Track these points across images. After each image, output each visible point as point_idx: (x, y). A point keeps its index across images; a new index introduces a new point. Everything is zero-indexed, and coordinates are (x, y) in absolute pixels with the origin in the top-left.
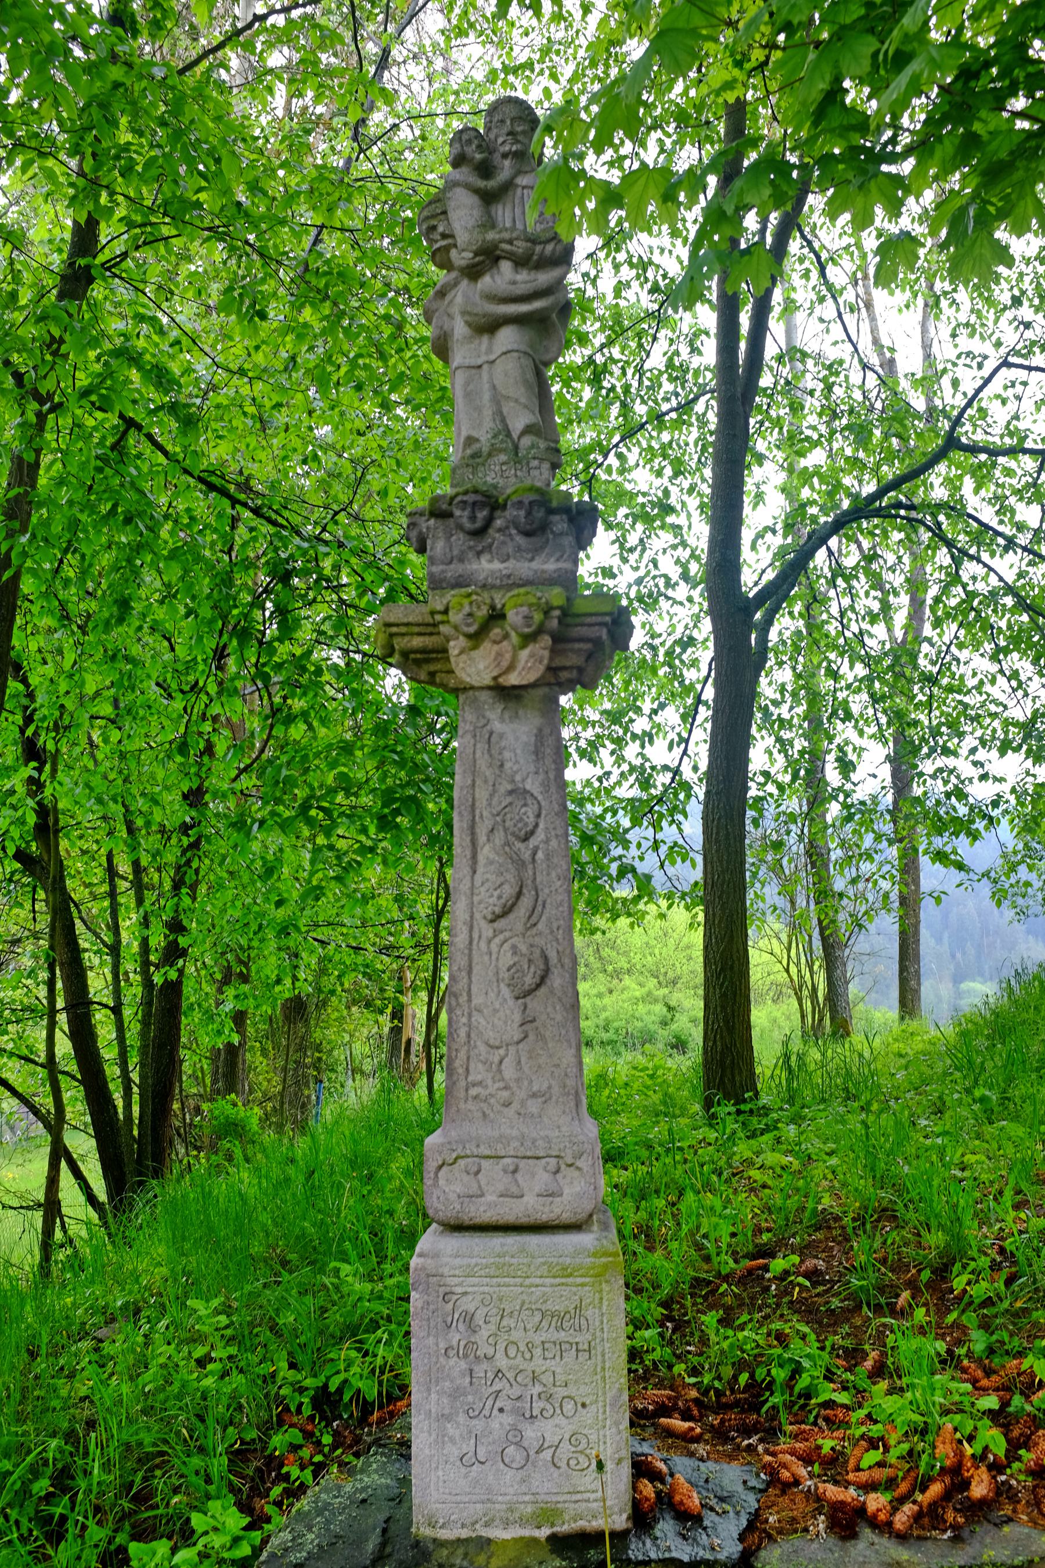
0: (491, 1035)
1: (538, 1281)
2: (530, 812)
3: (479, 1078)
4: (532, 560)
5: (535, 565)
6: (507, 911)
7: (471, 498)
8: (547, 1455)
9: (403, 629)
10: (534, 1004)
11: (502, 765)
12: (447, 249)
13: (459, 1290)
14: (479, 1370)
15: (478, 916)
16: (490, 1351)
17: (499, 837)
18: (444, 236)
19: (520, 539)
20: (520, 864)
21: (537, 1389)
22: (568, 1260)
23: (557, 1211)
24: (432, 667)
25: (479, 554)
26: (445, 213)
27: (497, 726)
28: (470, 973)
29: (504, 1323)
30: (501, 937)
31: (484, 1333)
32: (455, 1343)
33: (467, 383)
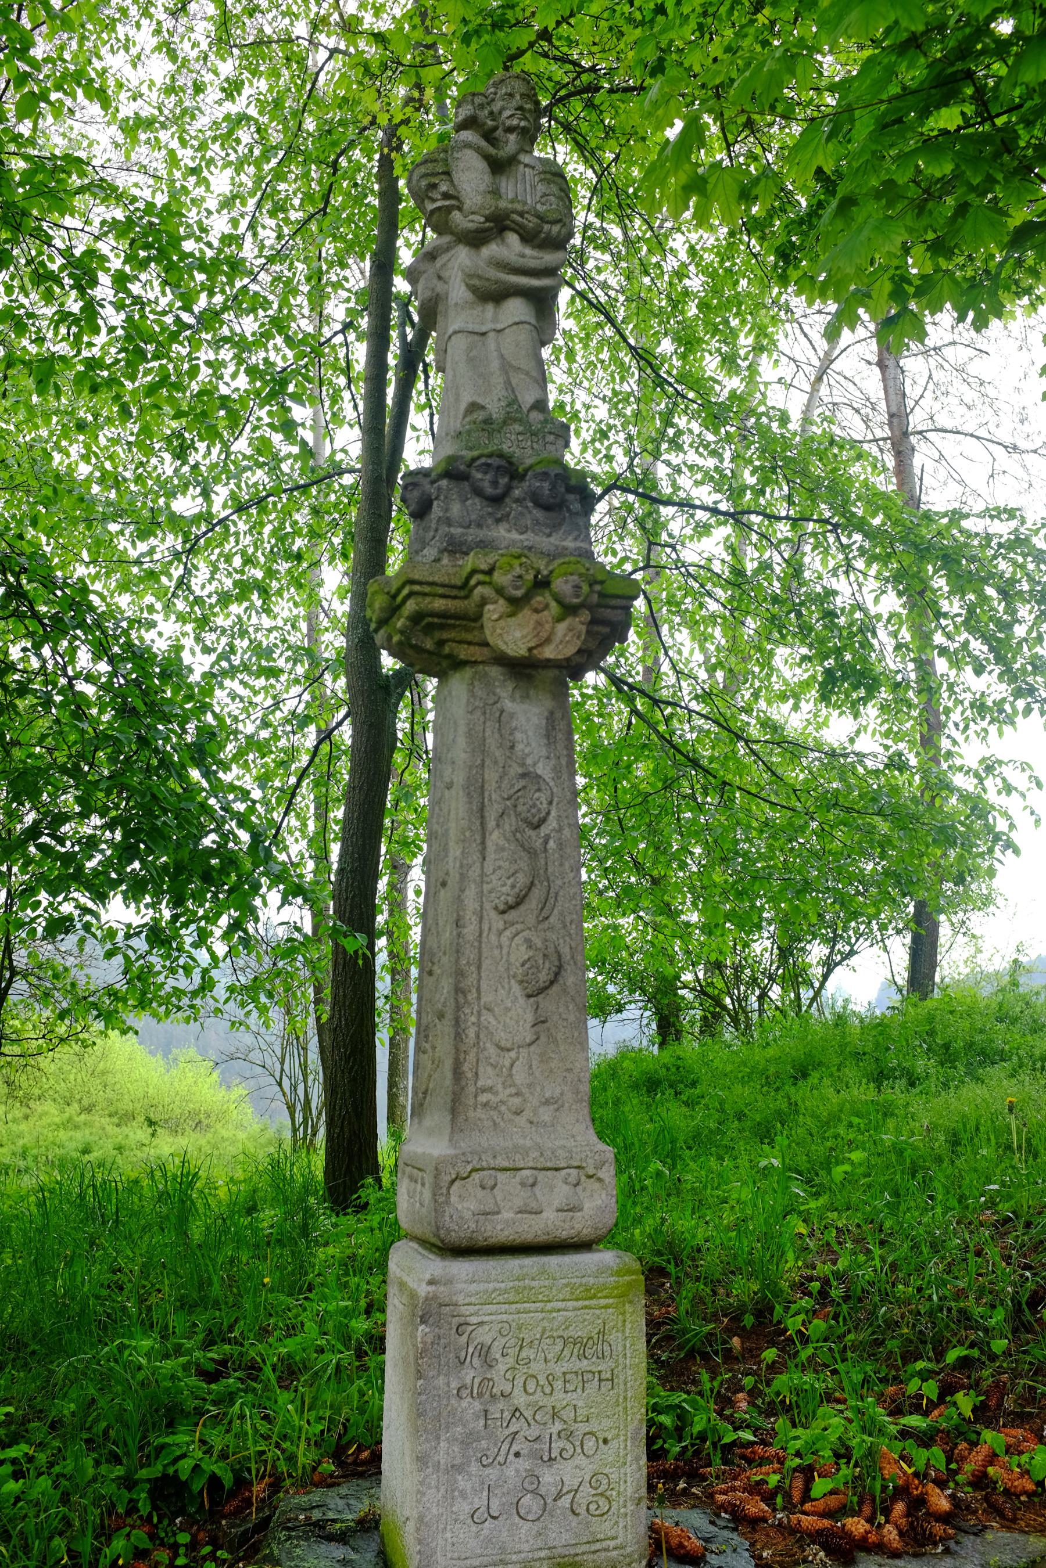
0: (502, 1037)
1: (560, 1305)
2: (543, 797)
3: (489, 1083)
4: (549, 535)
5: (552, 539)
6: (519, 902)
7: (495, 461)
8: (565, 1501)
9: (427, 589)
10: (548, 1003)
11: (512, 747)
12: (449, 210)
13: (474, 1320)
14: (495, 1412)
15: (488, 906)
16: (508, 1388)
17: (510, 823)
18: (446, 196)
19: (538, 513)
20: (532, 853)
21: (558, 1426)
22: (592, 1280)
23: (578, 1226)
24: (445, 635)
25: (498, 521)
26: (448, 173)
27: (508, 705)
28: (479, 968)
29: (523, 1354)
30: (513, 930)
31: (502, 1367)
32: (468, 1381)
33: (470, 348)
